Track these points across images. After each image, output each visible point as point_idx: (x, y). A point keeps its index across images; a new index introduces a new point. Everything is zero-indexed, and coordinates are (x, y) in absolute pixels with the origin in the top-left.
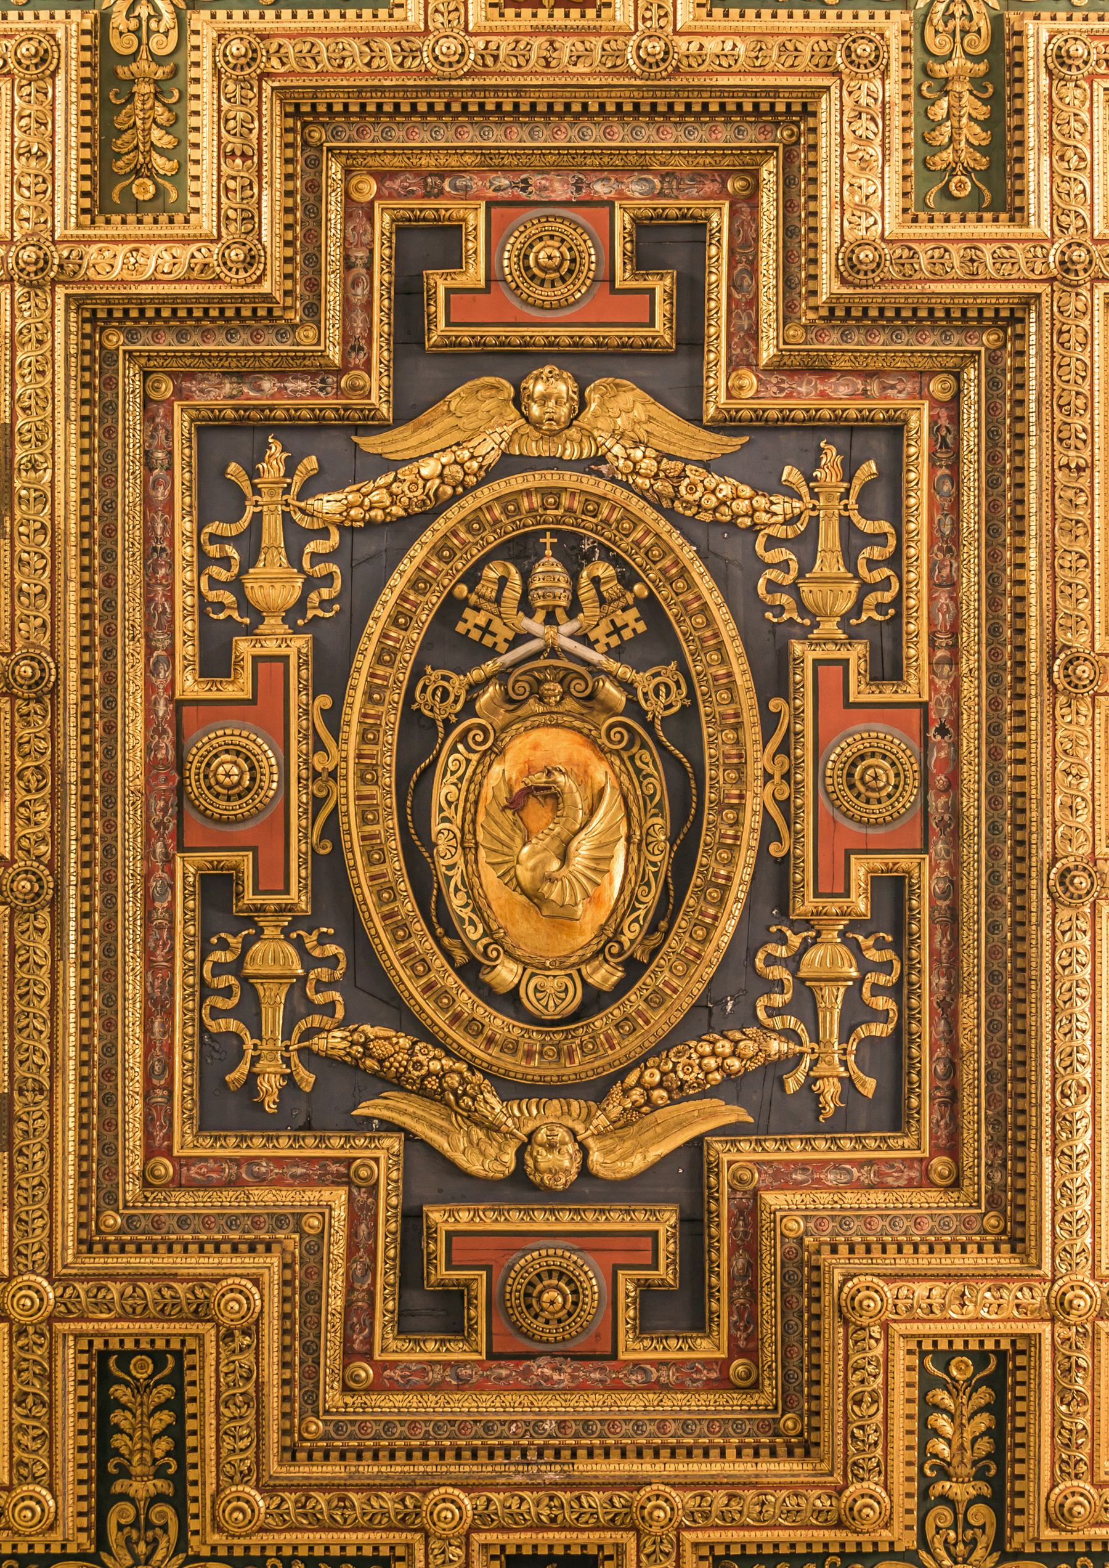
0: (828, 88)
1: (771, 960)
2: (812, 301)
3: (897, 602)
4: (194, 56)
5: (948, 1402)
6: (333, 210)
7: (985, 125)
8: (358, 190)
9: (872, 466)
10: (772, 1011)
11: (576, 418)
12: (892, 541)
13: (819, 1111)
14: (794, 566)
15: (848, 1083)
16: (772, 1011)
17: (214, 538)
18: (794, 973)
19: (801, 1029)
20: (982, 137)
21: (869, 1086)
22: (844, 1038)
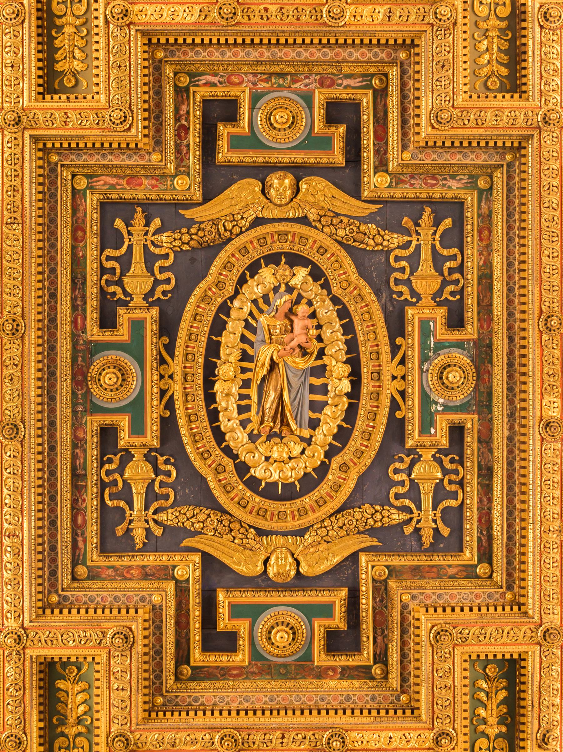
0: (426, 31)
1: (396, 471)
2: (417, 138)
3: (462, 292)
4: (95, 14)
5: (485, 686)
6: (169, 93)
7: (506, 52)
8: (180, 81)
9: (448, 222)
10: (397, 496)
11: (295, 197)
12: (459, 258)
13: (422, 545)
14: (408, 270)
15: (436, 530)
16: (397, 496)
17: (109, 258)
18: (409, 475)
19: (413, 506)
20: (505, 58)
21: (445, 531)
22: (435, 508)
